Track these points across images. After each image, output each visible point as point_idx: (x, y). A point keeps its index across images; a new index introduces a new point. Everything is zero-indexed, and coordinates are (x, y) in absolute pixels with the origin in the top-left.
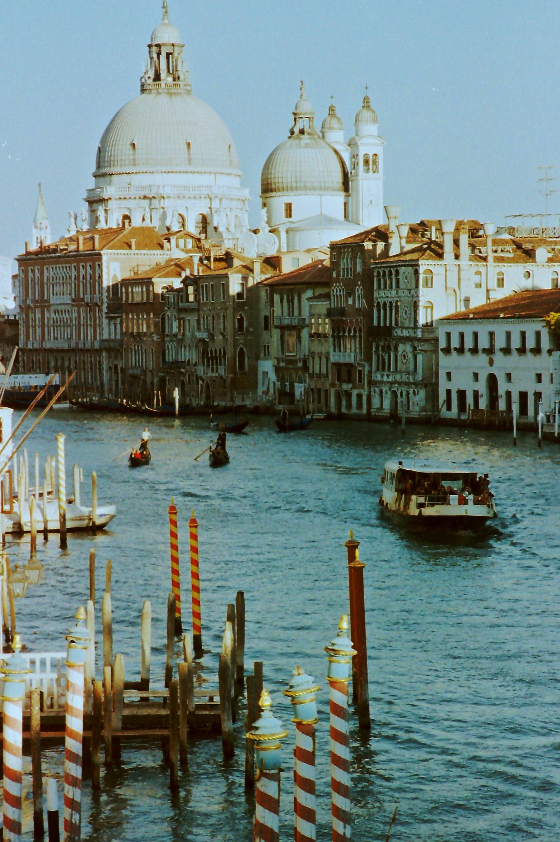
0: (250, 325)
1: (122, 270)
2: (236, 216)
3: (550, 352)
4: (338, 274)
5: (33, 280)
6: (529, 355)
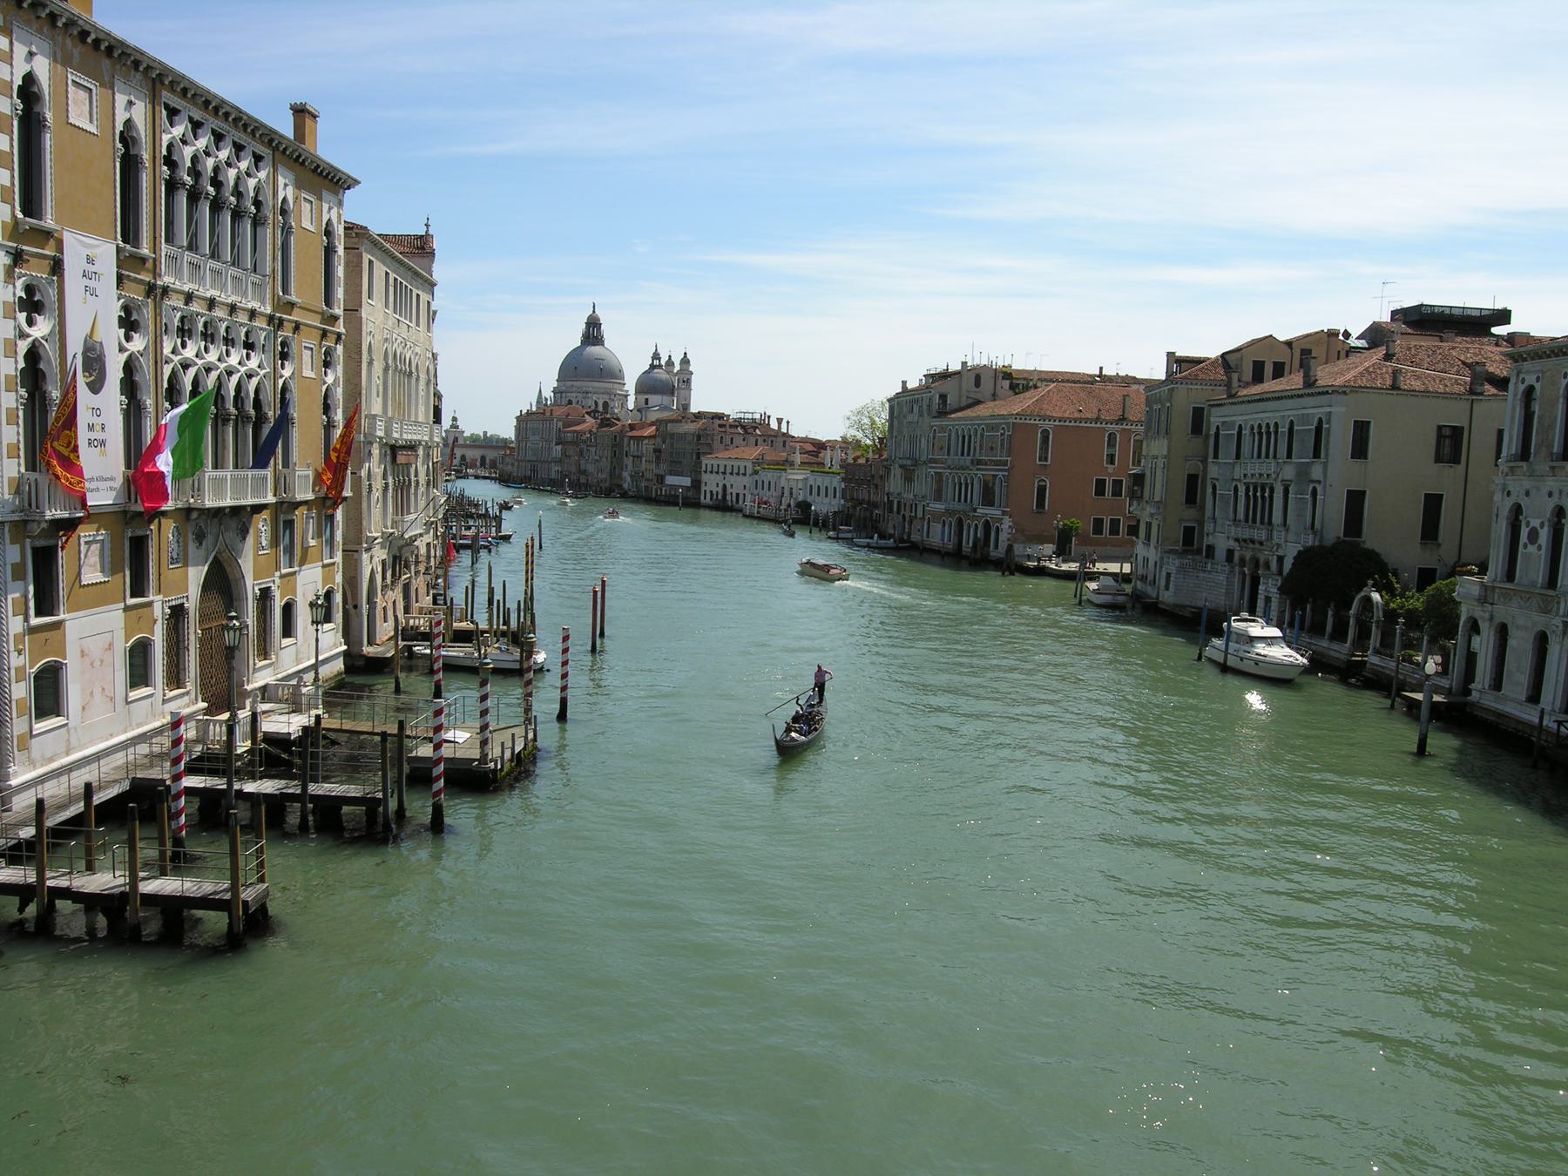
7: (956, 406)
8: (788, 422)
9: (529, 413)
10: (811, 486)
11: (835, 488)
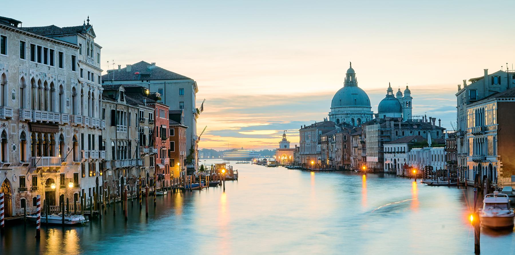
0: (348, 147)
1: (323, 133)
2: (369, 119)
3: (407, 152)
4: (363, 132)
5: (303, 136)
6: (403, 153)
7: (482, 97)
8: (440, 120)
9: (306, 128)
10: (432, 155)
11: (442, 155)
